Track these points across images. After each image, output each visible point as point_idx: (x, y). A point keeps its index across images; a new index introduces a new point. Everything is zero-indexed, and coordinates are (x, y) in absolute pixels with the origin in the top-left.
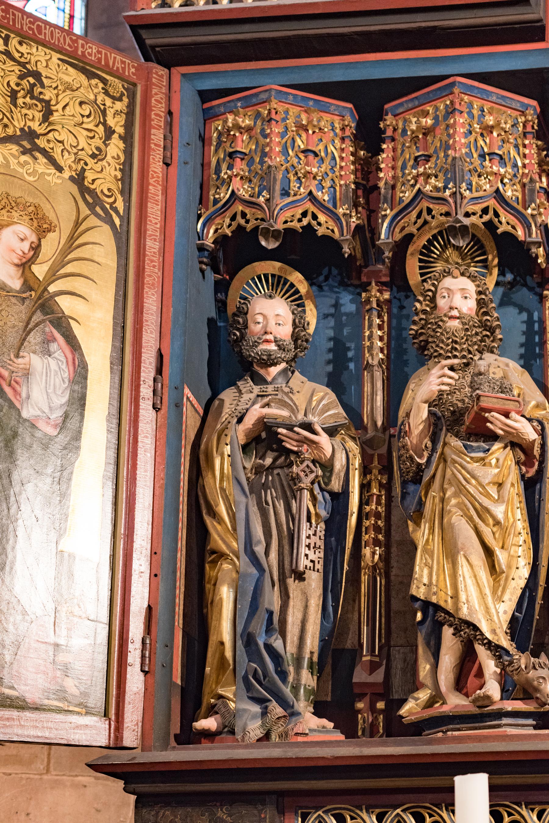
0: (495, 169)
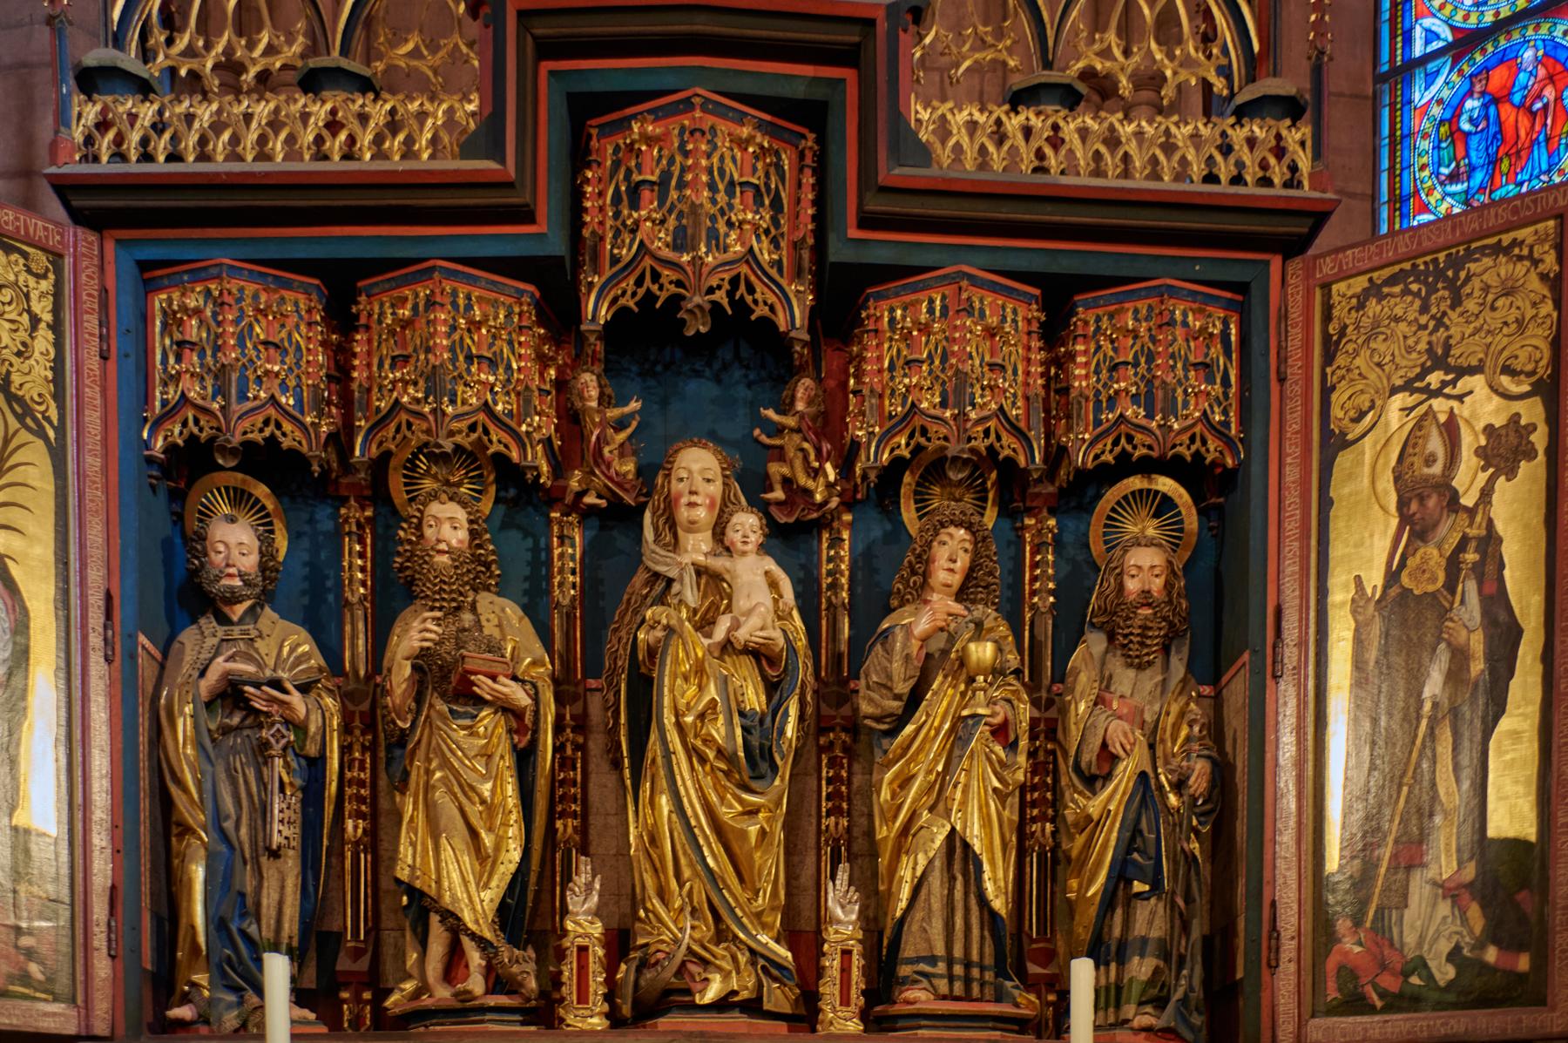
0: (483, 376)
